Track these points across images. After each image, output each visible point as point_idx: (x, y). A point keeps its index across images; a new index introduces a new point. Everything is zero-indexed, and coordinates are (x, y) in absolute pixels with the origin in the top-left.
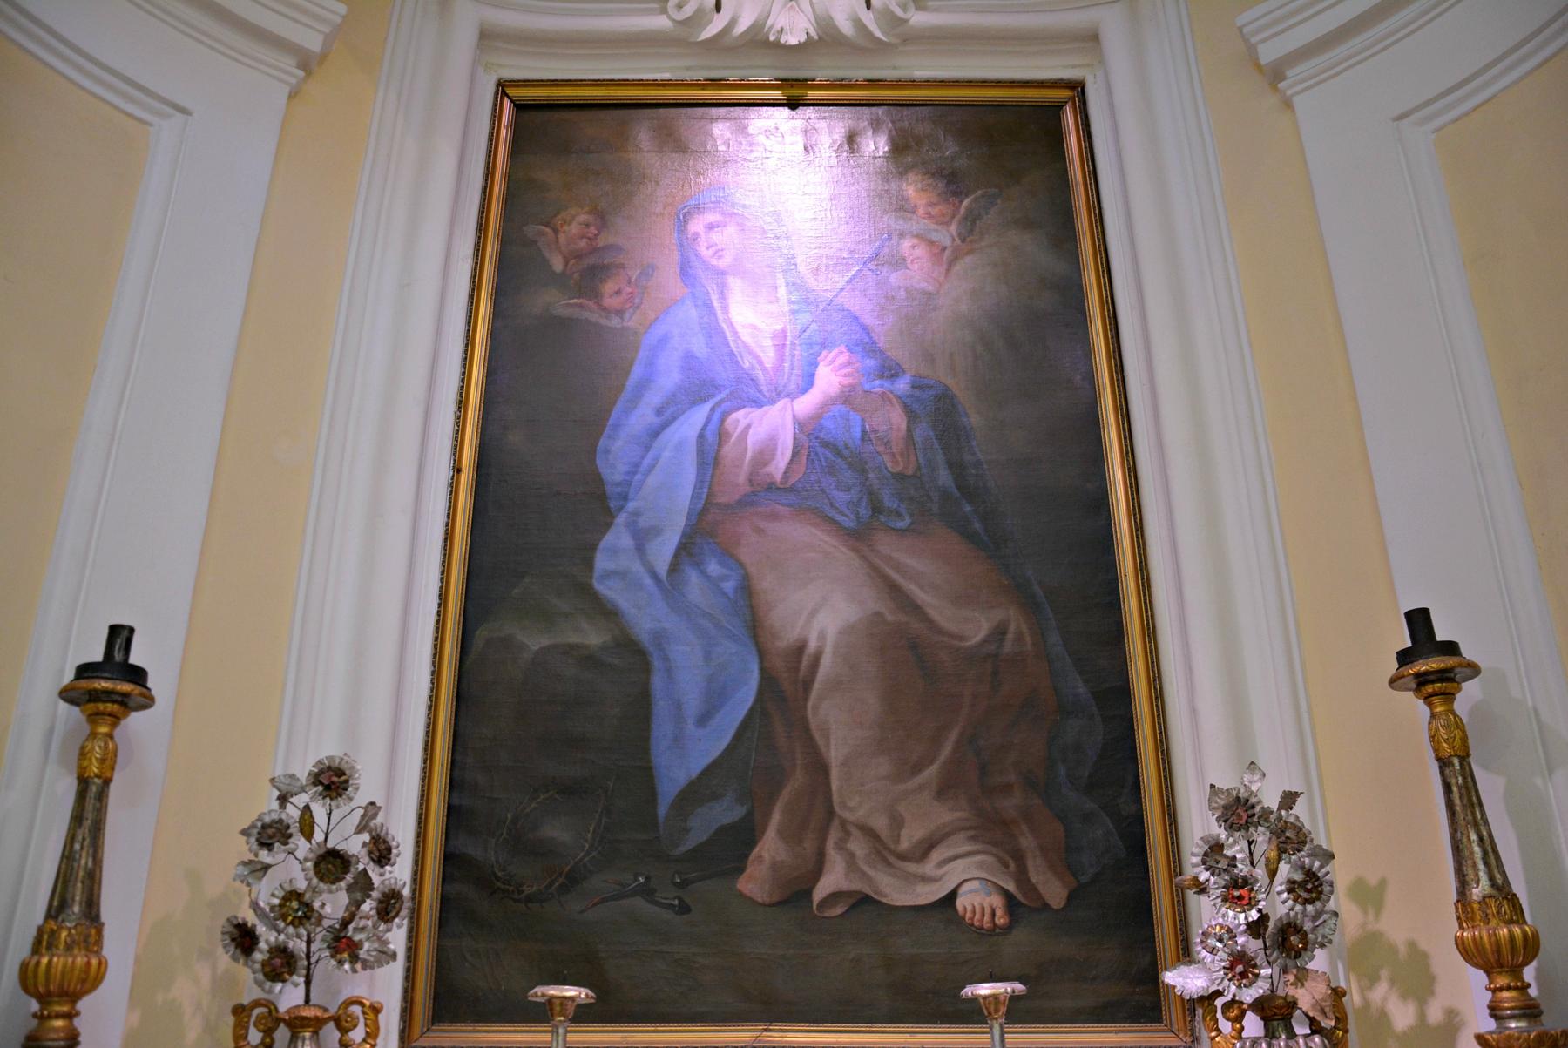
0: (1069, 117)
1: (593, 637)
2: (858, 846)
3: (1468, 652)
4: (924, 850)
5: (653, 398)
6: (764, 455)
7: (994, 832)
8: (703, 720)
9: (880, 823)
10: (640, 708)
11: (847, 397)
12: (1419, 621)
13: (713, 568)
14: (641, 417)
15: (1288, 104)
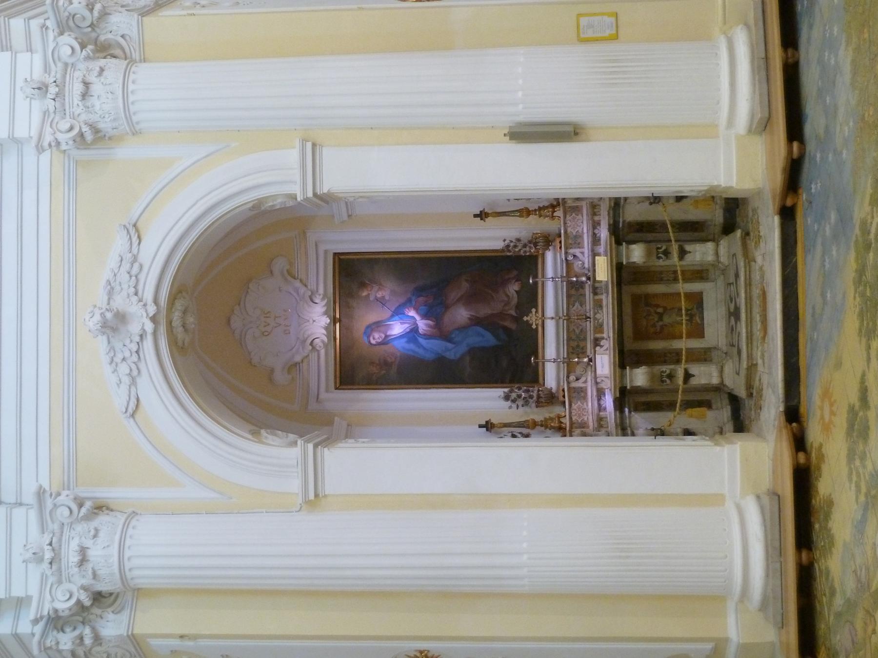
0: (342, 257)
1: (468, 358)
2: (507, 308)
4: (508, 296)
7: (505, 283)
8: (483, 336)
9: (503, 304)
10: (483, 349)
11: (417, 310)
12: (476, 216)
13: (453, 336)
14: (421, 351)
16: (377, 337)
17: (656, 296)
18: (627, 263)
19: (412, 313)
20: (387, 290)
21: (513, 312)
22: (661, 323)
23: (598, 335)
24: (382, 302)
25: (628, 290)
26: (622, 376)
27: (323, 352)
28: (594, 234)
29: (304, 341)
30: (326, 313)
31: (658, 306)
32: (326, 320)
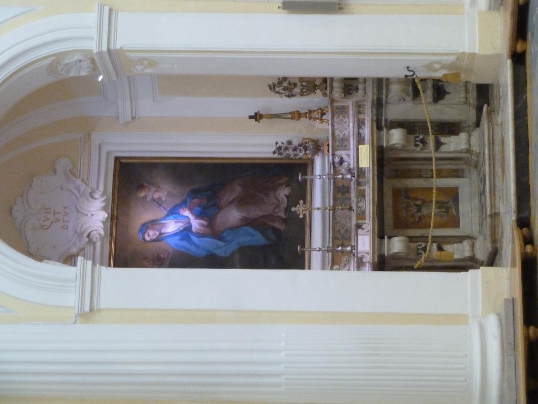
0: (123, 161)
1: (237, 256)
2: (277, 210)
3: (256, 111)
4: (278, 200)
5: (189, 246)
6: (202, 225)
7: (275, 188)
8: (253, 236)
9: (273, 207)
11: (191, 210)
12: (250, 117)
13: (225, 234)
14: (193, 248)
15: (140, 118)
16: (151, 234)
17: (415, 189)
18: (387, 147)
19: (186, 213)
20: (164, 191)
21: (282, 214)
22: (419, 214)
23: (360, 221)
24: (158, 202)
25: (390, 184)
26: (381, 246)
27: (98, 245)
28: (359, 134)
29: (81, 234)
30: (104, 209)
31: (417, 199)
32: (104, 215)
